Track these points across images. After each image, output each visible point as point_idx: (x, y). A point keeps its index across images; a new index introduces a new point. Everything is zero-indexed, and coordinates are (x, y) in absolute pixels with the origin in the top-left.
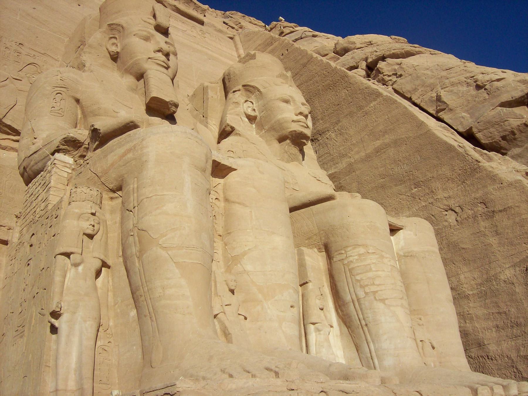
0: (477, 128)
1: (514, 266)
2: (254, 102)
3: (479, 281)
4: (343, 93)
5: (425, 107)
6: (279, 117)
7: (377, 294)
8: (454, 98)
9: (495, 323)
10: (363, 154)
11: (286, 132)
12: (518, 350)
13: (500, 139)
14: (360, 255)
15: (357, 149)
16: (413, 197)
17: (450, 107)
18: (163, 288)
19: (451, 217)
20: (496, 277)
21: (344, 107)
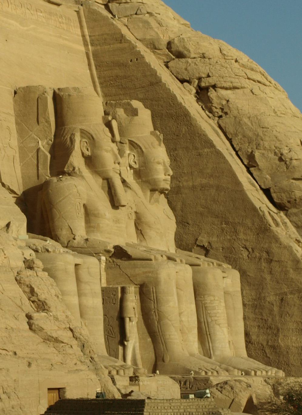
0: (273, 189)
1: (276, 295)
2: (136, 156)
3: (254, 297)
4: (184, 129)
5: (241, 157)
6: (155, 177)
7: (217, 322)
8: (264, 161)
9: (258, 324)
10: (191, 184)
11: (156, 188)
12: (268, 342)
13: (286, 202)
14: (211, 301)
15: (186, 178)
16: (223, 230)
17: (259, 167)
18: (170, 335)
19: (245, 254)
20: (264, 298)
21: (182, 139)
